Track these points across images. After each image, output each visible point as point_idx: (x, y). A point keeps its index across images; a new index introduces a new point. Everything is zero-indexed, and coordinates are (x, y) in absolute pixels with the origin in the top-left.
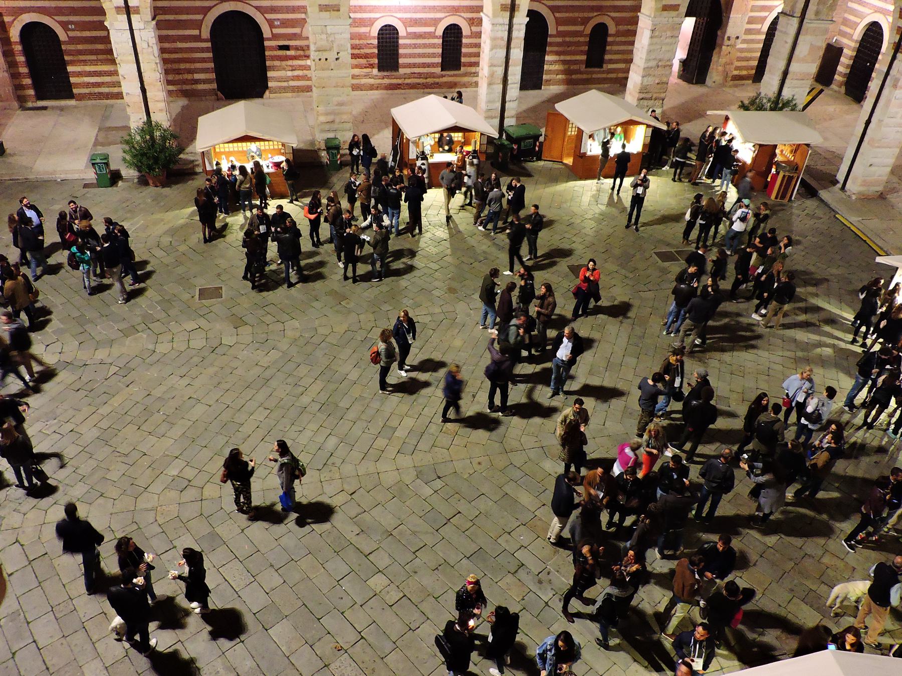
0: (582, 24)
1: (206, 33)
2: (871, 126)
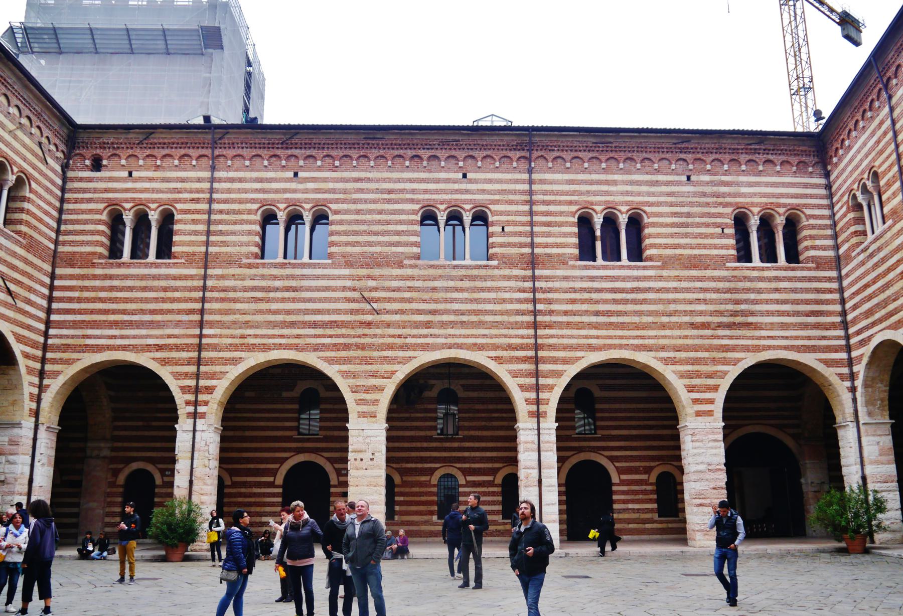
0: (645, 473)
1: (279, 480)
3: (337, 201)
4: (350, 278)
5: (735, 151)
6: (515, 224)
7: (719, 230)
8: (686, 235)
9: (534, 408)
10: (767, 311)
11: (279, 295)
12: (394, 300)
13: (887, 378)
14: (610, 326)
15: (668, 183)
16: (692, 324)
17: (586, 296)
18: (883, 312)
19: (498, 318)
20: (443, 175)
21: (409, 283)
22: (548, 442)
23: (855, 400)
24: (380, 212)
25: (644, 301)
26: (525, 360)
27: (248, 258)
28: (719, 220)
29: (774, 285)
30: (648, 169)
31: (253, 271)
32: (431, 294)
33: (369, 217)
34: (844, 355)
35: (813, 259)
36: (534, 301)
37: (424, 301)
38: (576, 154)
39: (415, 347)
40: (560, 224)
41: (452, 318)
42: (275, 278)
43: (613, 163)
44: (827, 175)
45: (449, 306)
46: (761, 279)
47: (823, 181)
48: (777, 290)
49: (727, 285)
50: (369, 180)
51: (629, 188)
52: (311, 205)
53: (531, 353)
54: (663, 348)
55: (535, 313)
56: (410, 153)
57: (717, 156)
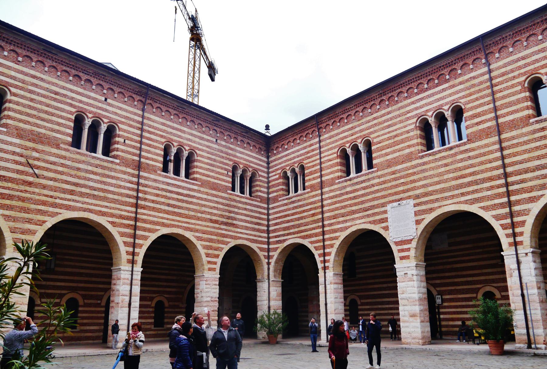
2: (328, 305)
3: (16, 87)
4: (20, 146)
5: (236, 133)
6: (132, 140)
7: (226, 172)
8: (213, 171)
9: (130, 257)
10: (241, 219)
13: (284, 260)
14: (174, 213)
15: (208, 141)
16: (211, 220)
17: (164, 193)
18: (296, 230)
19: (116, 197)
20: (92, 95)
21: (62, 161)
22: (136, 280)
23: (269, 269)
24: (48, 106)
25: (191, 203)
26: (128, 226)
28: (227, 167)
29: (244, 206)
30: (200, 130)
34: (266, 246)
35: (260, 197)
36: (138, 191)
37: (71, 176)
38: (168, 109)
39: (61, 206)
40: (156, 148)
41: (88, 191)
43: (185, 121)
44: (268, 157)
45: (87, 183)
46: (240, 202)
47: (266, 159)
48: (245, 209)
49: (227, 202)
50: (42, 80)
51: (190, 137)
53: (132, 223)
54: (197, 231)
55: (137, 198)
56: (74, 72)
57: (229, 133)
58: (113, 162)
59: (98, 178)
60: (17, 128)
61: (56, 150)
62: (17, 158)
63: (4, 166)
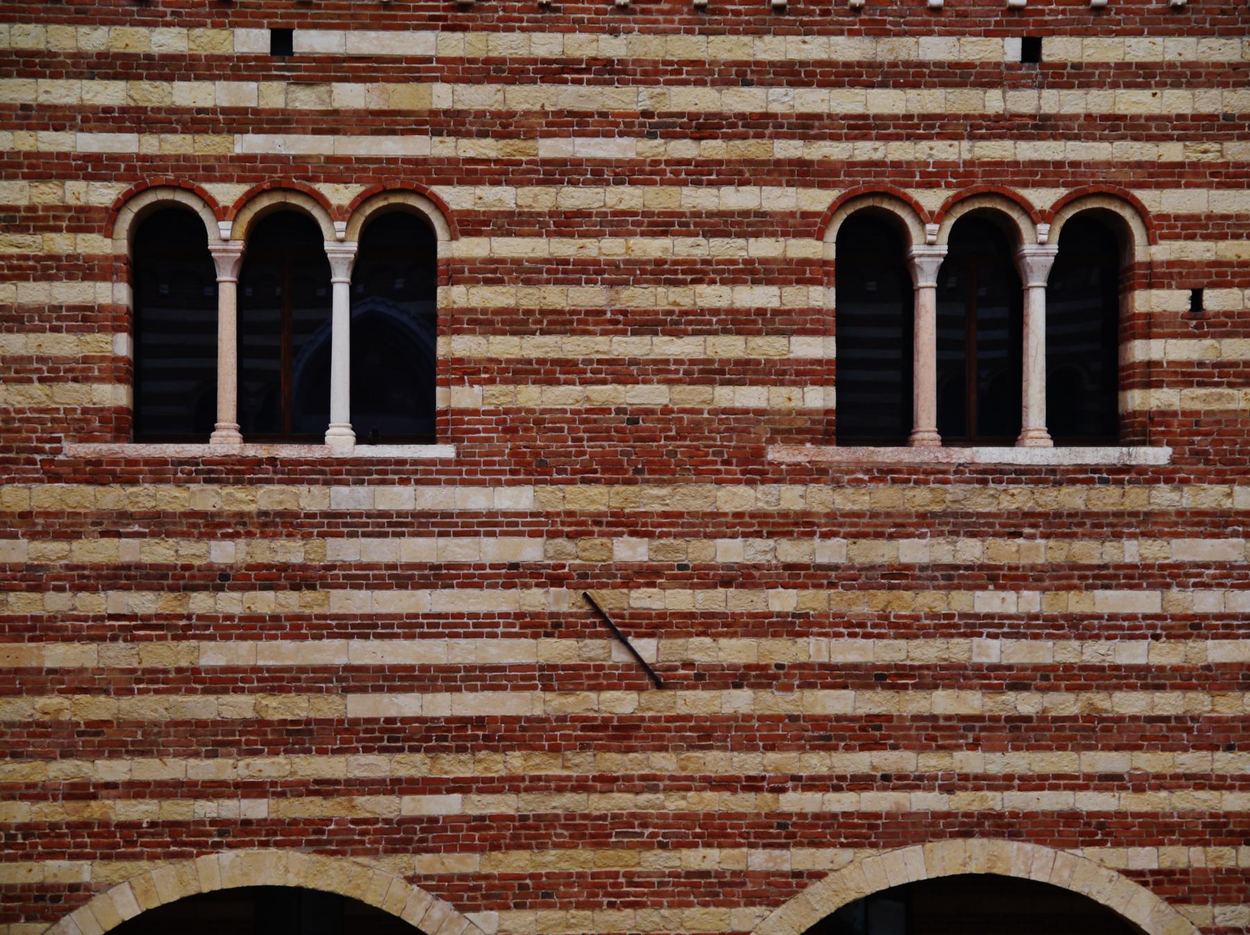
4: (536, 524)
11: (231, 603)
12: (729, 625)
19: (1169, 703)
21: (791, 551)
27: (86, 437)
31: (112, 497)
32: (882, 596)
33: (612, 248)
37: (856, 628)
41: (973, 702)
42: (209, 525)
45: (959, 650)
50: (607, 71)
52: (356, 189)
58: (1127, 469)
59: (1031, 601)
60: (512, 423)
61: (742, 489)
62: (536, 599)
63: (471, 659)
